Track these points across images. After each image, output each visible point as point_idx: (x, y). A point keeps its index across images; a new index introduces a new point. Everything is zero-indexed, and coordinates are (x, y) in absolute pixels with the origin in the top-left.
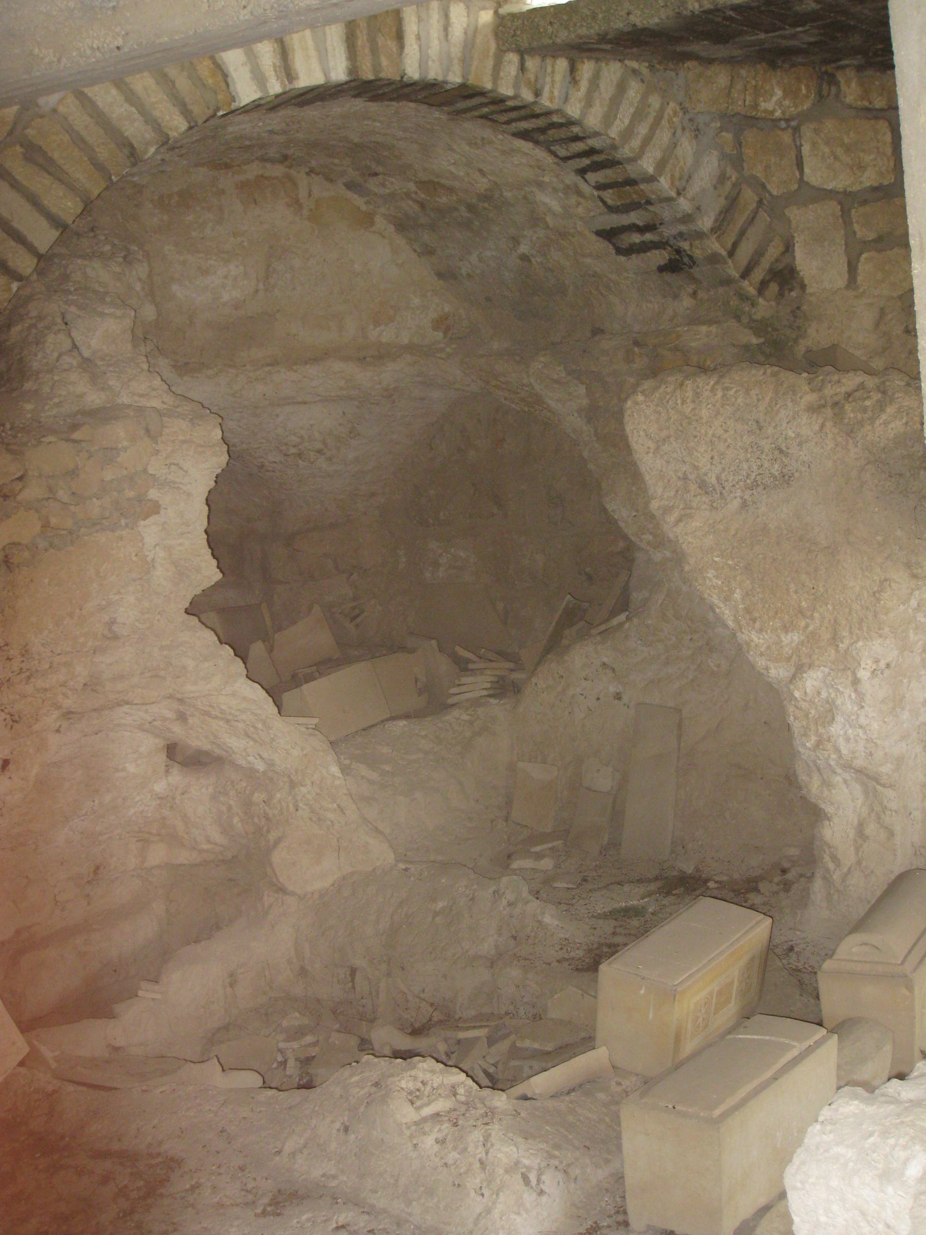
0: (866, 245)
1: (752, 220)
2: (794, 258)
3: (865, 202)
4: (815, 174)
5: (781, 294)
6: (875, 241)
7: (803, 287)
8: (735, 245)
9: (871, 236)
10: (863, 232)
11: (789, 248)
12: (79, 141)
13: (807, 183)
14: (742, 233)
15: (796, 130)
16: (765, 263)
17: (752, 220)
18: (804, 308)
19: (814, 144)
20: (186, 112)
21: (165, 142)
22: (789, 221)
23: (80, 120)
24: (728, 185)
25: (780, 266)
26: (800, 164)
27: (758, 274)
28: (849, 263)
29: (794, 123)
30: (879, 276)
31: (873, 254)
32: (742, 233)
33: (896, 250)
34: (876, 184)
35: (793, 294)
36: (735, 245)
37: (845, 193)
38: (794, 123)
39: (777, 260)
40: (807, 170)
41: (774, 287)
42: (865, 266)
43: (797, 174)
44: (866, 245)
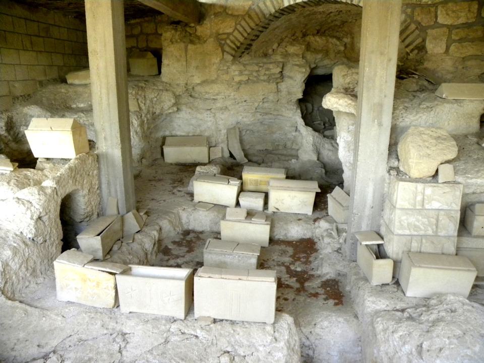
0: (455, 41)
1: (412, 32)
2: (425, 43)
3: (458, 28)
4: (441, 20)
5: (418, 53)
6: (459, 40)
7: (427, 52)
8: (405, 39)
9: (457, 38)
10: (454, 37)
11: (424, 40)
12: (257, 14)
13: (438, 23)
14: (408, 36)
15: (437, 7)
16: (415, 44)
17: (412, 32)
18: (425, 57)
19: (441, 11)
20: (275, 8)
21: (271, 14)
22: (427, 33)
23: (257, 10)
24: (407, 23)
25: (419, 45)
26: (436, 17)
27: (411, 47)
28: (447, 46)
29: (436, 5)
30: (456, 50)
31: (457, 44)
32: (408, 36)
33: (467, 43)
34: (464, 22)
35: (422, 53)
36: (405, 39)
37: (451, 25)
38: (436, 5)
39: (419, 44)
40: (438, 19)
41: (416, 51)
42: (452, 48)
43: (434, 20)
44: (455, 41)
